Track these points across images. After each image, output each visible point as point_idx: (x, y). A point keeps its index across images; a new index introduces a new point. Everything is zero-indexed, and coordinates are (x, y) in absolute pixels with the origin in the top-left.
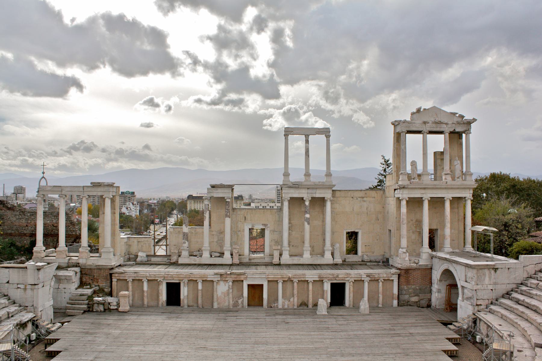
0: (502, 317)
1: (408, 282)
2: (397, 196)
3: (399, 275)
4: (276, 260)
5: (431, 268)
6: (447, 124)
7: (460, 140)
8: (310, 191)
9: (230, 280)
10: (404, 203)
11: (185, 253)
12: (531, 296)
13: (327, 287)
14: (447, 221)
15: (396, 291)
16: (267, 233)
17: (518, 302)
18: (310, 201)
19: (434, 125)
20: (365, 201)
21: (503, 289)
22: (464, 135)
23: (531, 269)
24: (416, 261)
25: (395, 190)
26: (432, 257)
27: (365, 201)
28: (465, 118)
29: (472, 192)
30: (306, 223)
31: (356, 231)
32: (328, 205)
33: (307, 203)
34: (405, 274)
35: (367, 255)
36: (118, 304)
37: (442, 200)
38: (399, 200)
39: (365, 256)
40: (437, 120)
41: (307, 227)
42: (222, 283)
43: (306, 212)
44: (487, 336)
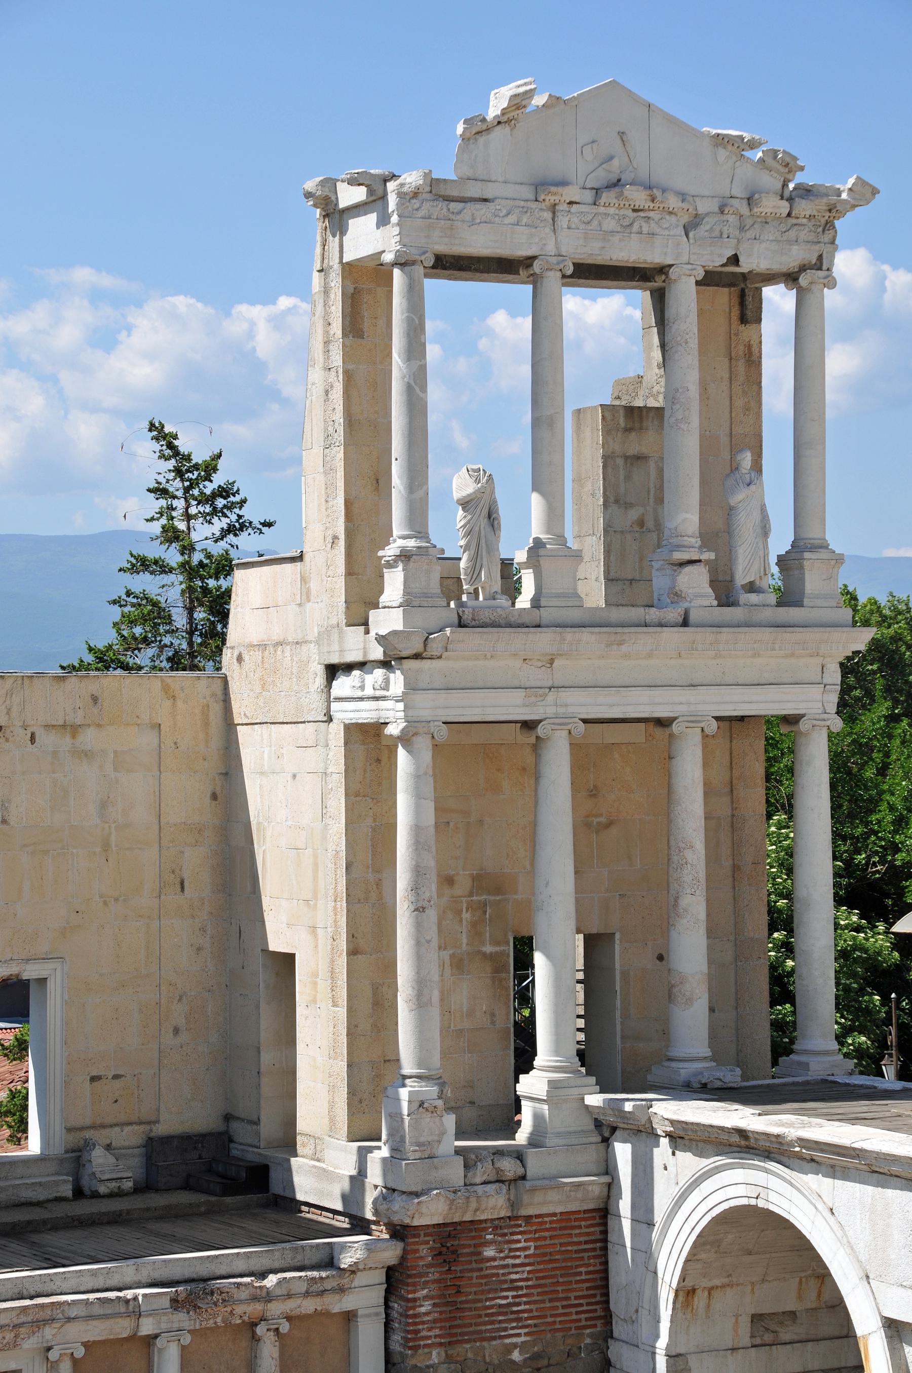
2: (345, 713)
7: (746, 331)
14: (687, 876)
20: (86, 755)
22: (778, 300)
25: (333, 671)
27: (86, 755)
28: (800, 178)
31: (30, 972)
35: (108, 1147)
39: (99, 1159)
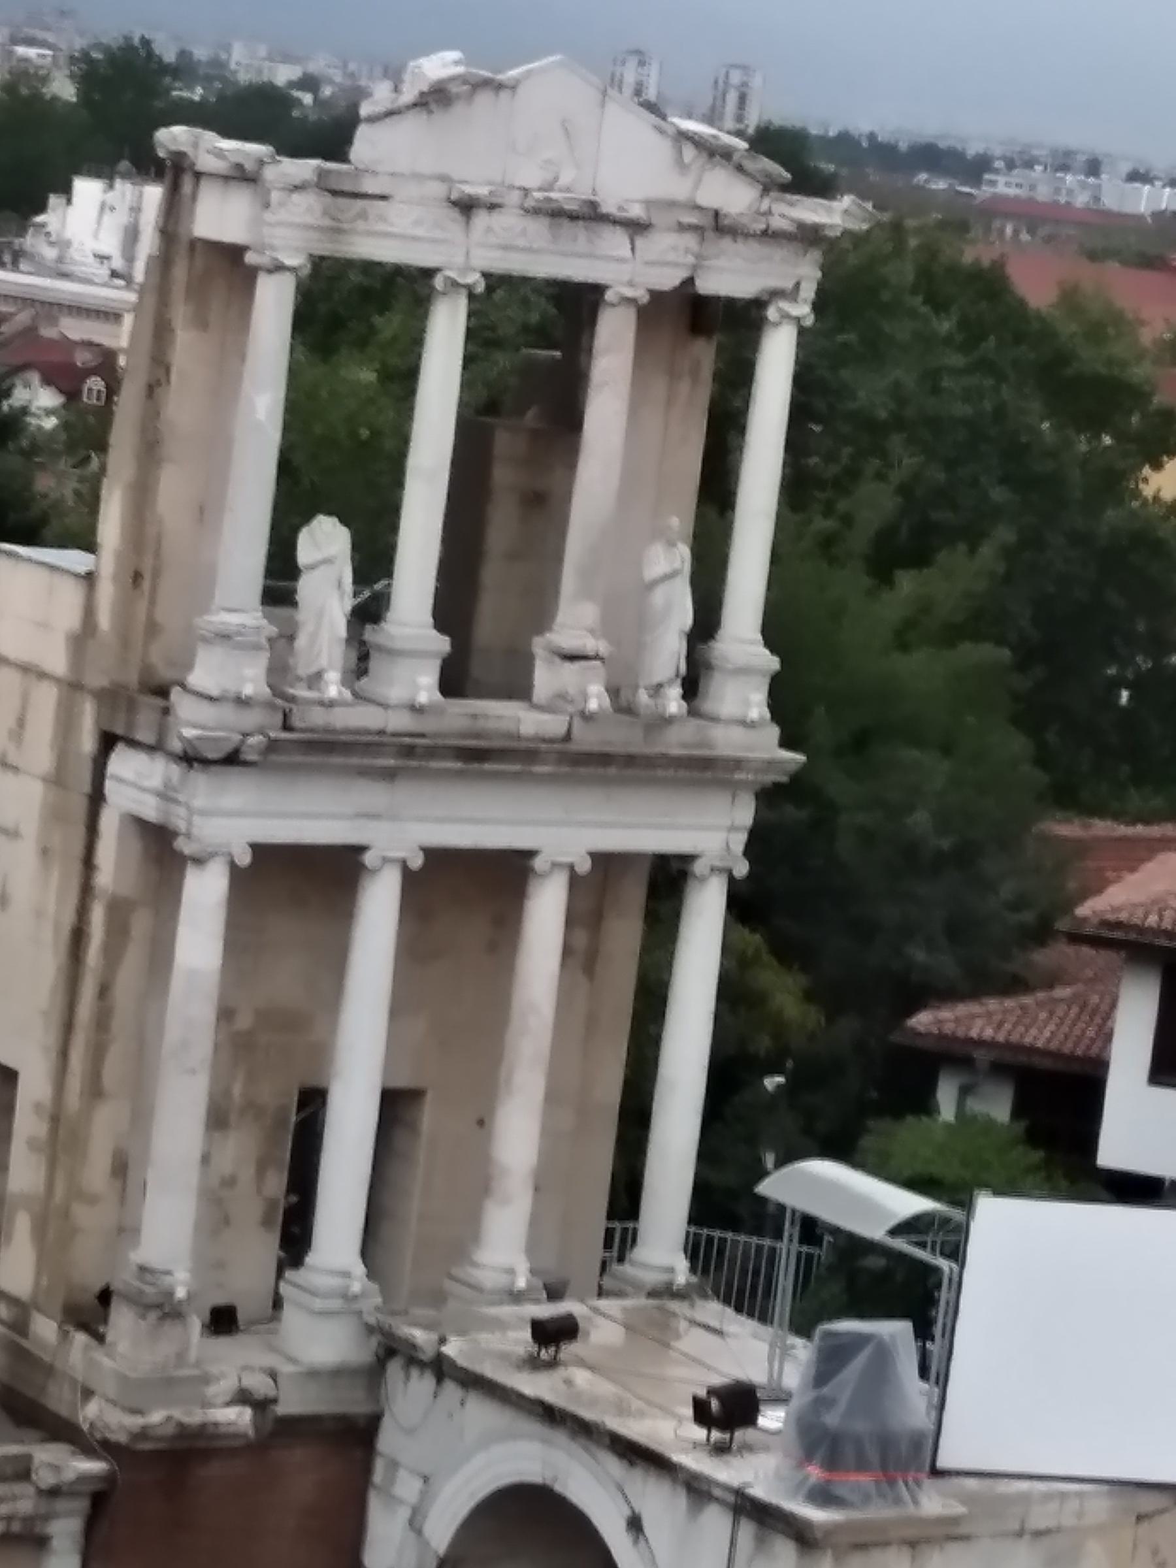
6: (636, 228)
10: (205, 894)
19: (538, 228)
24: (260, 1385)
29: (745, 813)
37: (499, 878)
40: (574, 184)
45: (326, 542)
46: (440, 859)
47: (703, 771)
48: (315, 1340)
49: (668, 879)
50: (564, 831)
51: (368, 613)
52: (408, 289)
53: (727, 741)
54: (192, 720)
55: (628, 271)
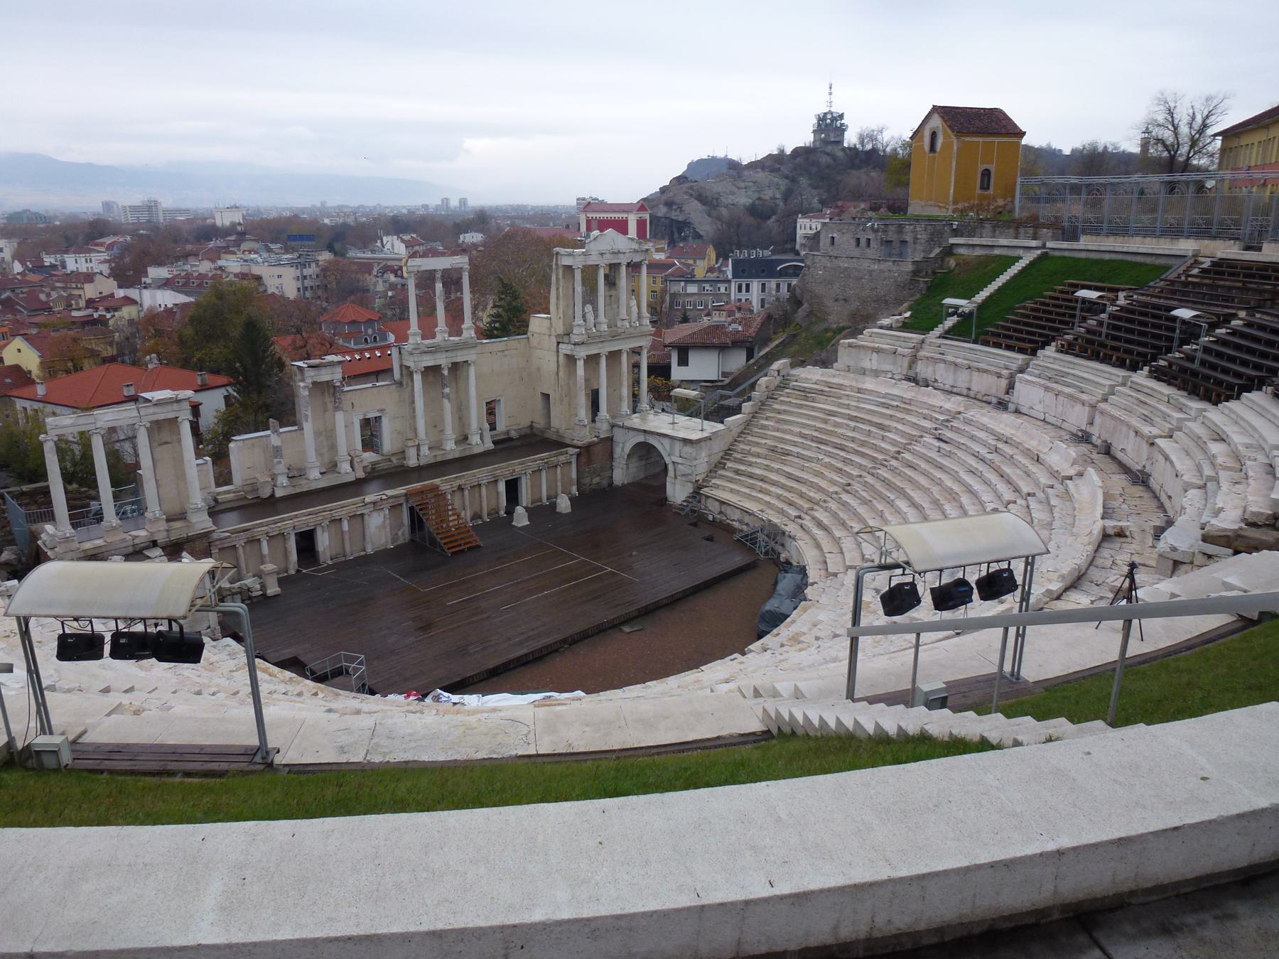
0: (732, 491)
1: (589, 462)
3: (578, 455)
4: (412, 462)
5: (610, 440)
8: (449, 354)
9: (386, 506)
10: (580, 364)
11: (282, 480)
12: (750, 464)
13: (502, 487)
15: (574, 475)
16: (385, 423)
17: (737, 472)
18: (449, 369)
21: (717, 458)
23: (736, 431)
26: (613, 426)
30: (446, 402)
32: (472, 370)
33: (446, 372)
34: (586, 452)
36: (263, 587)
38: (571, 359)
41: (447, 404)
42: (375, 514)
43: (444, 386)
44: (721, 513)
45: (589, 308)
46: (610, 353)
47: (643, 335)
48: (603, 428)
49: (636, 352)
50: (626, 346)
51: (596, 317)
52: (596, 267)
53: (645, 329)
54: (575, 339)
55: (624, 260)
